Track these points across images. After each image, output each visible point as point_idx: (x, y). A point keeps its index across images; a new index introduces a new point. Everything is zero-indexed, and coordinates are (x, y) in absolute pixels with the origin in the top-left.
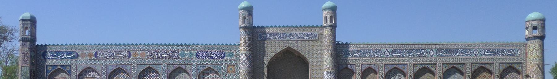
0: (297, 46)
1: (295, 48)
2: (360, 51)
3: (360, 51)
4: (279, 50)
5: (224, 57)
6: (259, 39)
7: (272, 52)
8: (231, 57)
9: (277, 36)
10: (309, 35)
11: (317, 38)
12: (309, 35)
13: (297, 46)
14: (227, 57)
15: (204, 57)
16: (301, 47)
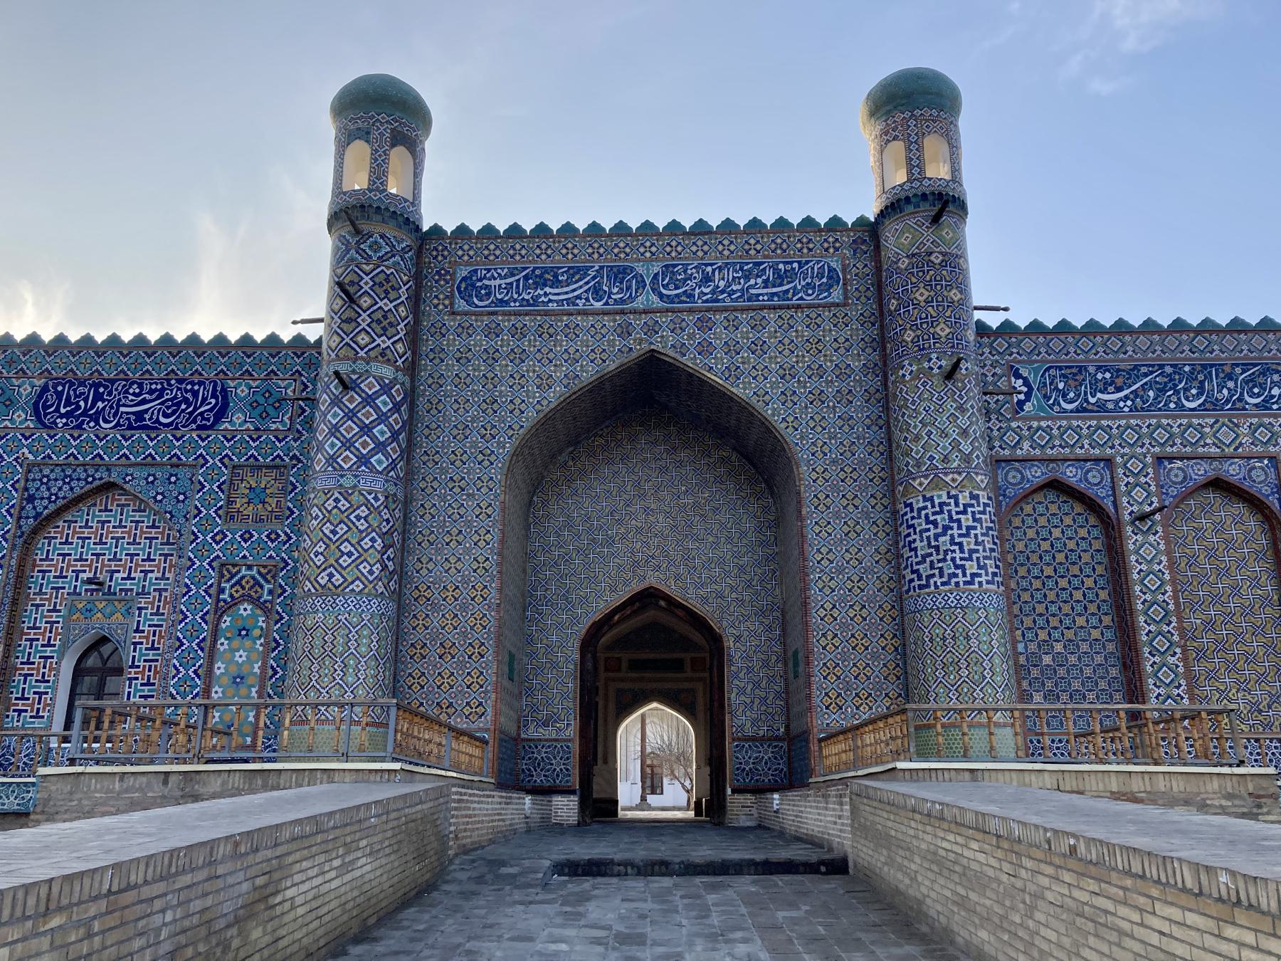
0: (705, 349)
1: (691, 361)
2: (1134, 373)
3: (1134, 373)
4: (588, 373)
5: (221, 413)
6: (461, 305)
7: (545, 383)
8: (265, 416)
9: (579, 288)
10: (780, 278)
11: (836, 295)
12: (789, 276)
13: (705, 349)
14: (237, 419)
15: (78, 419)
16: (732, 349)
